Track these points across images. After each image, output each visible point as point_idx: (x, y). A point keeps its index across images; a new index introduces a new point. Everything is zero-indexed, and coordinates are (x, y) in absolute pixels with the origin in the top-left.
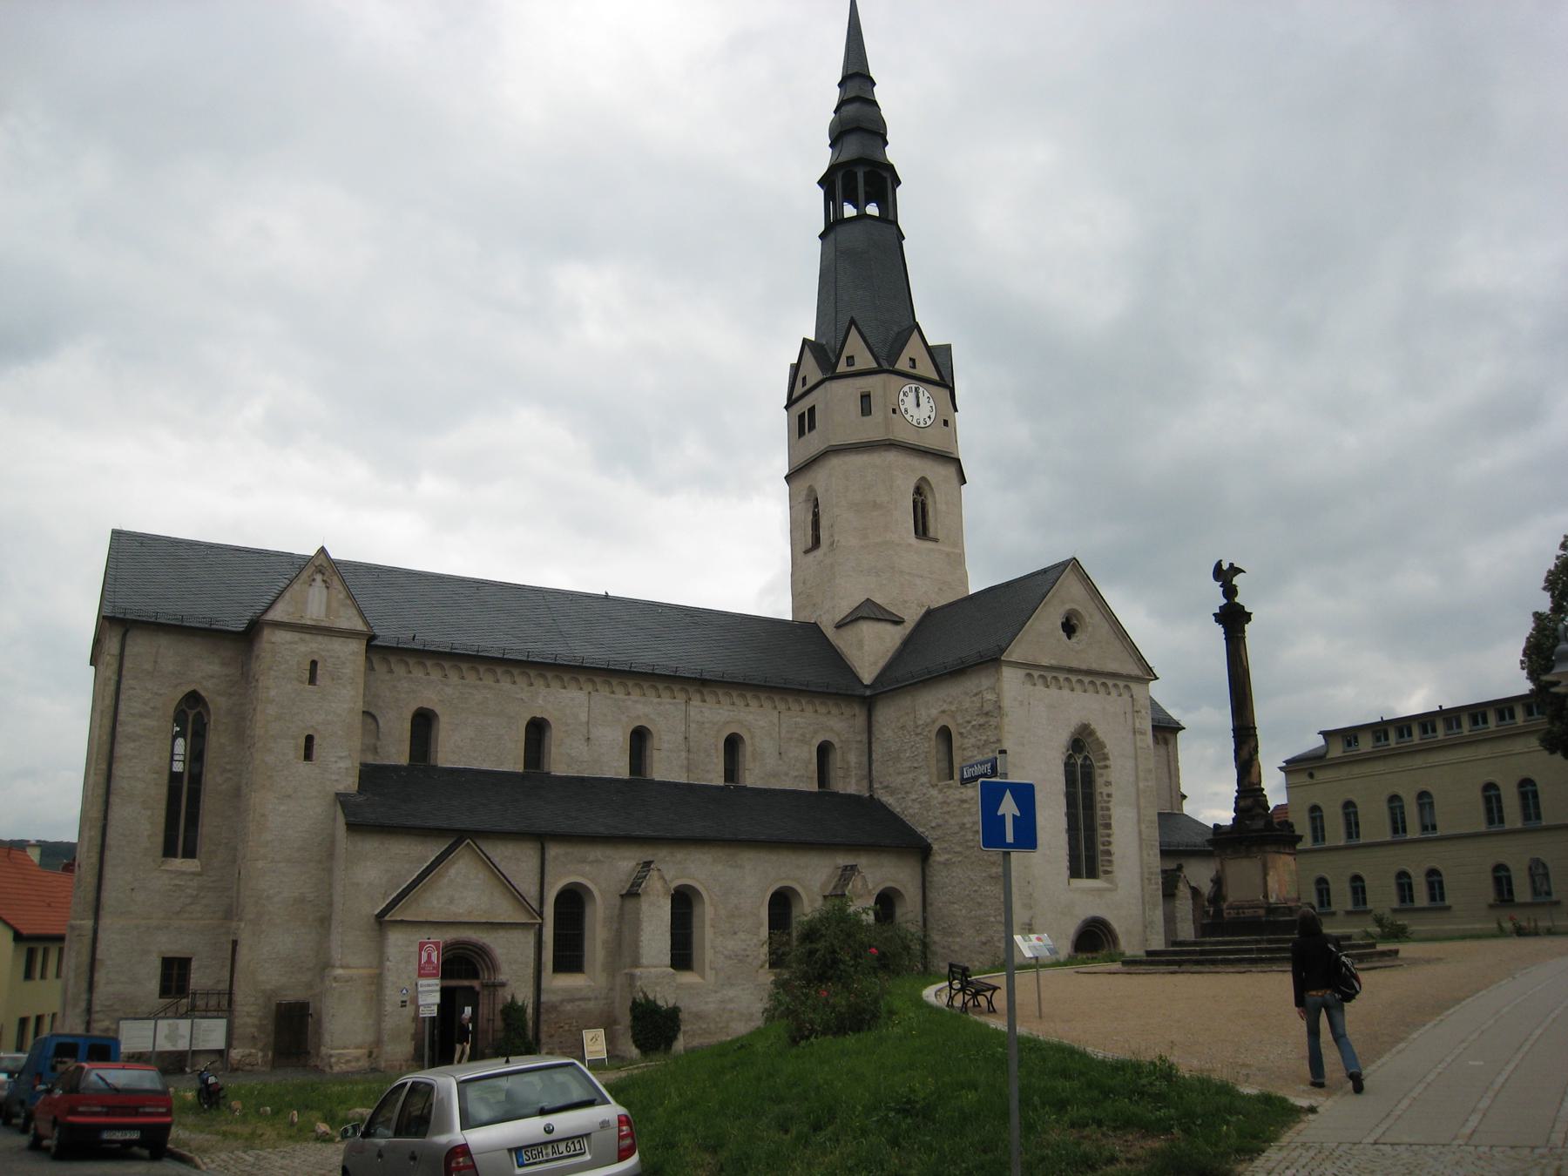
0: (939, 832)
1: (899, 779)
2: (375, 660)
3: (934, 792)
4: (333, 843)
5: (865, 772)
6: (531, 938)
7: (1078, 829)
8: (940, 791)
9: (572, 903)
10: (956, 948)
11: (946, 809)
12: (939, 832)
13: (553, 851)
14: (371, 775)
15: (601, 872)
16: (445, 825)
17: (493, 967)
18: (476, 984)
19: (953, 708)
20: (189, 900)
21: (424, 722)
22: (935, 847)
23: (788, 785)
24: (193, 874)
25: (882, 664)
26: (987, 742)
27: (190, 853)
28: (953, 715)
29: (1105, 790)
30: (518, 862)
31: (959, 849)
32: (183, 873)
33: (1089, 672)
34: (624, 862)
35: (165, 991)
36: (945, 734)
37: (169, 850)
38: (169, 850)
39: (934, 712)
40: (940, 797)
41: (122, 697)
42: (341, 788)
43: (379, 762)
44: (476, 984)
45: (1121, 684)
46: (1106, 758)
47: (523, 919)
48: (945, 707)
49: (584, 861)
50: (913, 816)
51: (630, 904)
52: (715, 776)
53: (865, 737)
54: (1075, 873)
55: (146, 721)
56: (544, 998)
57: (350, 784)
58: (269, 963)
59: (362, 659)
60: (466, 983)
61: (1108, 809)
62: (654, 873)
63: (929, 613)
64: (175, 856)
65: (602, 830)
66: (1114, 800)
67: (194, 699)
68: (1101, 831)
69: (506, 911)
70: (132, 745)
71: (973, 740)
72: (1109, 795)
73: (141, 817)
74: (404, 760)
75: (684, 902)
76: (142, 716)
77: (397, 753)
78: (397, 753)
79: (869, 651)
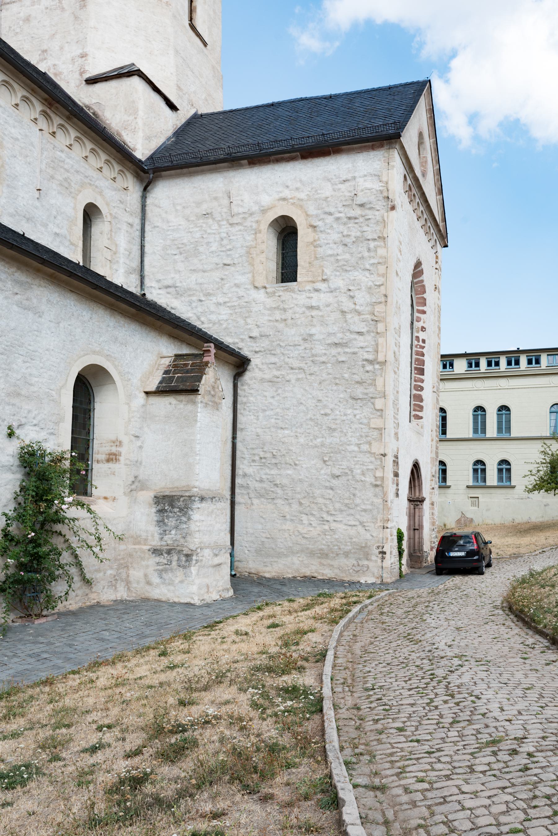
0: (264, 344)
1: (194, 277)
3: (260, 295)
5: (136, 263)
8: (270, 295)
10: (285, 481)
11: (278, 315)
12: (264, 344)
19: (303, 196)
22: (256, 361)
26: (360, 239)
28: (299, 204)
31: (296, 364)
39: (266, 200)
40: (270, 302)
48: (287, 193)
50: (219, 323)
53: (137, 222)
71: (336, 237)
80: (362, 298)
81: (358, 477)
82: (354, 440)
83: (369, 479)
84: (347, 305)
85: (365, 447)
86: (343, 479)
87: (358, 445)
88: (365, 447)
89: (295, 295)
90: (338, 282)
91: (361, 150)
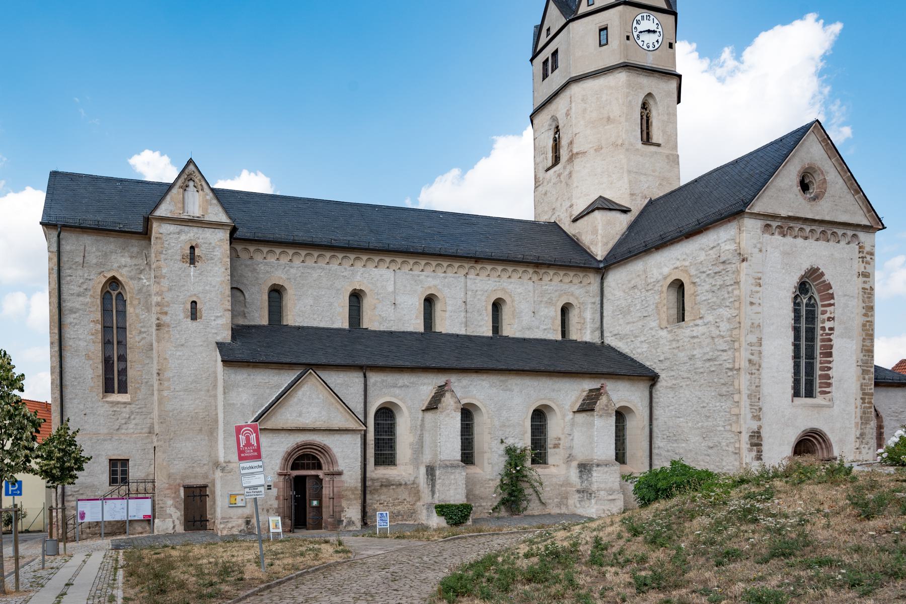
2: (239, 248)
4: (216, 377)
6: (358, 439)
7: (799, 358)
14: (238, 332)
15: (408, 393)
16: (294, 361)
18: (320, 473)
20: (123, 422)
24: (125, 403)
27: (123, 389)
29: (828, 325)
30: (350, 384)
32: (118, 403)
33: (822, 222)
37: (108, 388)
38: (108, 388)
41: (63, 282)
42: (219, 339)
43: (247, 323)
49: (395, 386)
51: (429, 415)
54: (796, 394)
55: (81, 299)
56: (368, 483)
57: (225, 336)
58: (180, 461)
59: (227, 246)
61: (831, 340)
62: (448, 395)
64: (113, 392)
66: (836, 332)
67: (114, 282)
68: (818, 358)
69: (341, 420)
70: (74, 316)
72: (831, 329)
73: (87, 368)
75: (467, 413)
76: (79, 295)
81: (724, 448)
82: (721, 423)
83: (731, 449)
85: (728, 428)
86: (715, 450)
87: (724, 426)
88: (728, 428)
91: (722, 225)
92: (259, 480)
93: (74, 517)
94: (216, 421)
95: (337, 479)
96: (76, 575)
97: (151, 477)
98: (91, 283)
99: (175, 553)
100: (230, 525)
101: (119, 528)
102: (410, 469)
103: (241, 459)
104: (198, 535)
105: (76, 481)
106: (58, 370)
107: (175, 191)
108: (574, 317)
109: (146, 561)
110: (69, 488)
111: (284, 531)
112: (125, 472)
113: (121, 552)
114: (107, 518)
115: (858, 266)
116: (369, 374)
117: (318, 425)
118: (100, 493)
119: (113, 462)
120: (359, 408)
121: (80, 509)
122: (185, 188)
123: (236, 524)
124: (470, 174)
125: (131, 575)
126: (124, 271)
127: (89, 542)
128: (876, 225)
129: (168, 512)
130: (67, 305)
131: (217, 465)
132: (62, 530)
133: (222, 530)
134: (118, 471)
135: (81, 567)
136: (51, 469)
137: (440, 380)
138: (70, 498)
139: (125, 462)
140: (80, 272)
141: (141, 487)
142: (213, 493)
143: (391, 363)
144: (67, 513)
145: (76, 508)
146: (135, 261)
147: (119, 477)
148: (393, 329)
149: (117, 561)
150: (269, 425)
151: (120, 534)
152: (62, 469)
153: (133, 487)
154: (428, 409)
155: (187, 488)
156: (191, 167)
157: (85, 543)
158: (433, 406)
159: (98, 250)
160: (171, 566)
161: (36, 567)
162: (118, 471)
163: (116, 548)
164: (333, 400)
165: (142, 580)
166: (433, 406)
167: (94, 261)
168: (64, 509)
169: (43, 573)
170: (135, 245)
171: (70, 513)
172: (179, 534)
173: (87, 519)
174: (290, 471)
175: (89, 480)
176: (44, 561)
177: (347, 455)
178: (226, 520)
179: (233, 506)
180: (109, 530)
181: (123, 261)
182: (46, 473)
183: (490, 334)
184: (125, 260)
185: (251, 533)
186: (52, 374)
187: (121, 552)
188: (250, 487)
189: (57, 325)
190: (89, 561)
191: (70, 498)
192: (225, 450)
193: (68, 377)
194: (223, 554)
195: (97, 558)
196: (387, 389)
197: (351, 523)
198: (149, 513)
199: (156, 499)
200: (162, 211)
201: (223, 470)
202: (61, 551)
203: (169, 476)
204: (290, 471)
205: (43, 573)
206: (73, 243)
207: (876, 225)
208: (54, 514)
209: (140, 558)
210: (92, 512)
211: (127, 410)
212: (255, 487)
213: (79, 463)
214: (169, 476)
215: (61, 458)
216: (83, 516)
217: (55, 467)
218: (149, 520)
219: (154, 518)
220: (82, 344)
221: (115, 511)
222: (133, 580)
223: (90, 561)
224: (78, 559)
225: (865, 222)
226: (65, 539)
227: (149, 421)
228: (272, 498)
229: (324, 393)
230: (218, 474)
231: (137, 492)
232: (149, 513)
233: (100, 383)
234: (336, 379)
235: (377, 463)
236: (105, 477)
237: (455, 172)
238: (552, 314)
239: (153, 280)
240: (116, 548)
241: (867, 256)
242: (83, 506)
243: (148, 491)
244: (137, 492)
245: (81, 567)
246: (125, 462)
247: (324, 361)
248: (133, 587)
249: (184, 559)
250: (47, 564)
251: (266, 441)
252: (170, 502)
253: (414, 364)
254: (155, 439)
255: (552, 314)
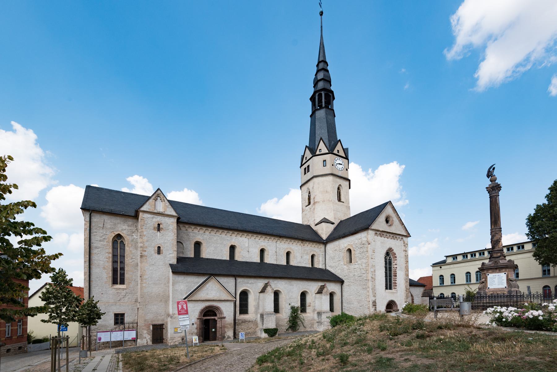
6: (232, 304)
9: (244, 295)
13: (239, 280)
15: (253, 286)
17: (221, 313)
21: (198, 245)
23: (303, 265)
25: (328, 235)
30: (229, 282)
34: (260, 283)
35: (116, 323)
36: (350, 251)
39: (346, 245)
44: (216, 318)
45: (401, 237)
46: (396, 257)
47: (230, 298)
51: (262, 294)
52: (284, 263)
60: (213, 318)
62: (269, 287)
63: (341, 221)
65: (253, 275)
74: (192, 256)
75: (277, 294)
77: (191, 254)
78: (191, 254)
79: (324, 231)
80: (364, 265)
84: (361, 267)
89: (352, 266)
90: (359, 262)
92: (187, 322)
93: (95, 340)
94: (169, 297)
95: (223, 320)
96: (98, 365)
97: (136, 321)
98: (107, 236)
99: (147, 354)
100: (174, 341)
101: (120, 343)
102: (254, 315)
103: (179, 314)
104: (159, 346)
105: (97, 324)
106: (88, 274)
107: (151, 200)
108: (316, 259)
109: (133, 358)
110: (93, 327)
111: (199, 342)
112: (123, 320)
113: (120, 354)
114: (113, 340)
115: (404, 248)
116: (237, 278)
117: (215, 298)
118: (109, 329)
119: (116, 315)
120: (233, 292)
121: (98, 336)
122: (156, 200)
123: (178, 340)
124: (281, 201)
125: (126, 364)
126: (124, 232)
127: (103, 351)
128: (408, 235)
129: (144, 336)
130: (93, 245)
131: (168, 315)
132: (89, 345)
133: (170, 342)
134: (119, 319)
135: (100, 362)
136: (84, 319)
137: (266, 281)
138: (93, 331)
139: (123, 315)
140: (101, 231)
141: (131, 325)
142: (167, 327)
143: (246, 274)
144: (92, 338)
145: (96, 336)
146: (130, 228)
147: (119, 321)
148: (248, 261)
149: (118, 358)
150: (193, 298)
151: (119, 346)
152: (89, 318)
153: (127, 326)
154: (261, 292)
155: (154, 326)
156: (159, 192)
157: (101, 351)
158: (263, 291)
159: (111, 222)
160: (146, 359)
161: (76, 363)
162: (119, 319)
163: (118, 353)
164: (222, 288)
165: (131, 365)
166: (263, 291)
167: (109, 227)
168: (90, 337)
169: (80, 365)
170: (130, 222)
171: (93, 338)
172: (150, 346)
173: (102, 340)
174: (202, 317)
175: (103, 323)
176: (80, 360)
177: (227, 311)
178: (172, 338)
179: (176, 332)
180: (114, 345)
181: (124, 227)
182: (80, 321)
183: (285, 264)
184: (125, 227)
185: (184, 344)
186: (85, 275)
187: (120, 354)
188: (183, 325)
189: (88, 254)
190: (104, 359)
191: (93, 331)
192: (172, 309)
193: (93, 277)
194: (170, 353)
195: (108, 358)
196: (244, 284)
197: (229, 337)
198: (135, 336)
199: (138, 330)
200: (144, 208)
201: (171, 317)
202: (89, 355)
203: (145, 321)
204: (202, 317)
205: (80, 365)
206: (97, 219)
207: (408, 235)
208: (85, 339)
209: (131, 357)
210: (105, 337)
211: (124, 291)
212: (185, 325)
213: (99, 316)
214: (145, 321)
215: (89, 313)
216: (100, 339)
217: (86, 318)
218: (134, 340)
219: (137, 339)
220: (102, 263)
221: (117, 336)
222: (127, 366)
223: (104, 359)
224: (97, 359)
225: (405, 234)
226: (90, 350)
227: (135, 297)
228: (195, 329)
229: (218, 286)
230: (169, 319)
231: (129, 328)
232: (135, 336)
233: (110, 280)
234: (223, 280)
235: (240, 313)
236: (112, 322)
237: (275, 199)
238: (308, 258)
239: (139, 236)
240: (118, 353)
241: (406, 245)
242: (99, 335)
243: (134, 327)
244: (129, 328)
245: (100, 362)
246: (123, 315)
247: (218, 273)
248: (127, 369)
249: (152, 356)
250: (82, 362)
251: (190, 305)
252: (145, 332)
253: (256, 275)
254: (138, 304)
255: (308, 258)
